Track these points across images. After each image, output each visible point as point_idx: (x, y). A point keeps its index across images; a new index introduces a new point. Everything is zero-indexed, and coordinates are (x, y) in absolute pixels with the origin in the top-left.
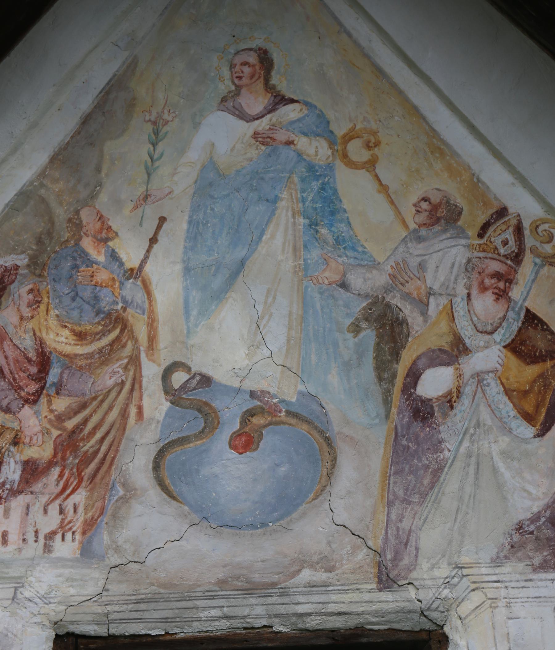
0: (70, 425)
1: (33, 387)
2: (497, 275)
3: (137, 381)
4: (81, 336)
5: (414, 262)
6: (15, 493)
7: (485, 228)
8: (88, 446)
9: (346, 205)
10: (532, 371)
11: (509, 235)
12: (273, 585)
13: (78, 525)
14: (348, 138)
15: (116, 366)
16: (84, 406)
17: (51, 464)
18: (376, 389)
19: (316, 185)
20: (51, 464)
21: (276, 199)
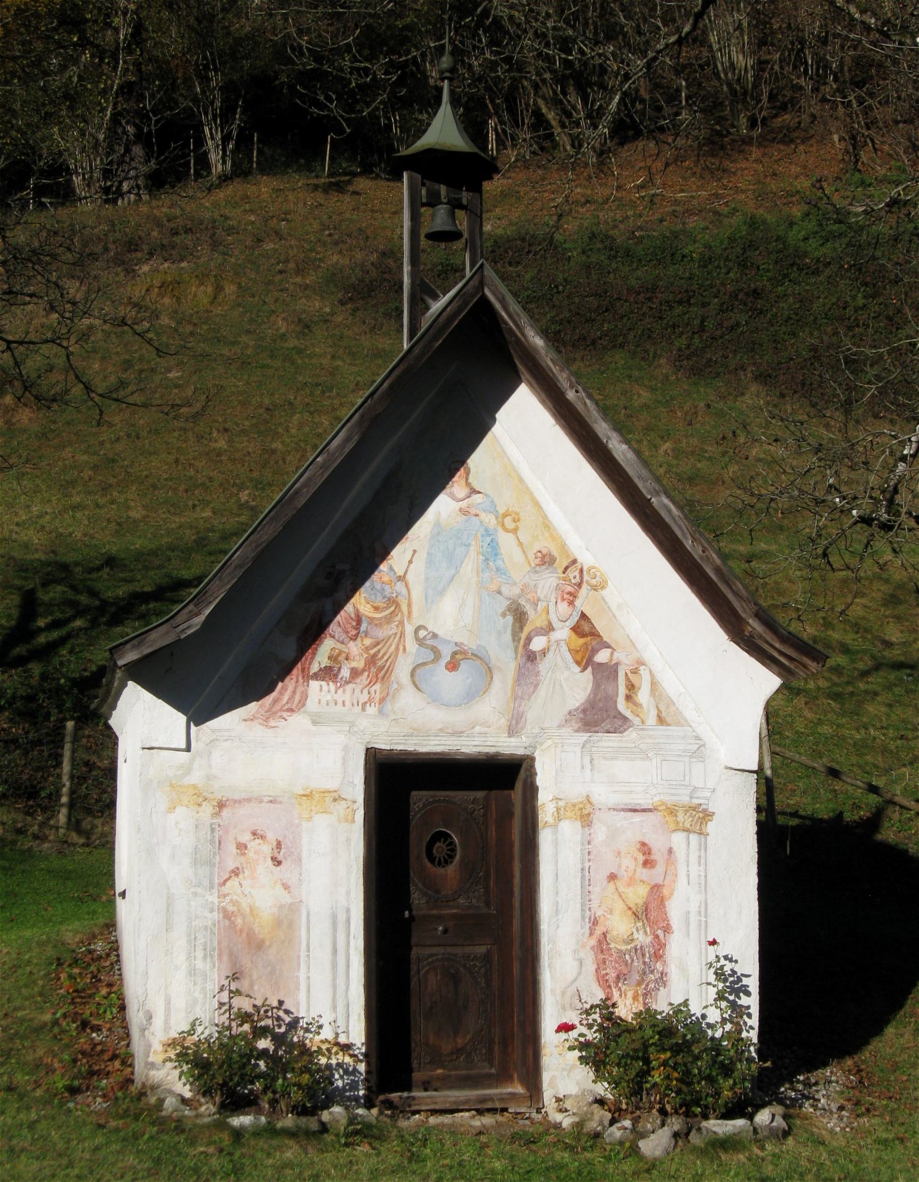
0: (372, 652)
1: (354, 632)
2: (570, 593)
3: (403, 634)
4: (376, 609)
5: (532, 584)
6: (347, 683)
7: (566, 568)
8: (380, 663)
9: (502, 551)
10: (581, 641)
11: (577, 573)
12: (462, 732)
13: (377, 700)
14: (505, 515)
15: (394, 625)
16: (378, 644)
17: (363, 670)
18: (511, 644)
19: (488, 539)
20: (363, 670)
21: (469, 545)
